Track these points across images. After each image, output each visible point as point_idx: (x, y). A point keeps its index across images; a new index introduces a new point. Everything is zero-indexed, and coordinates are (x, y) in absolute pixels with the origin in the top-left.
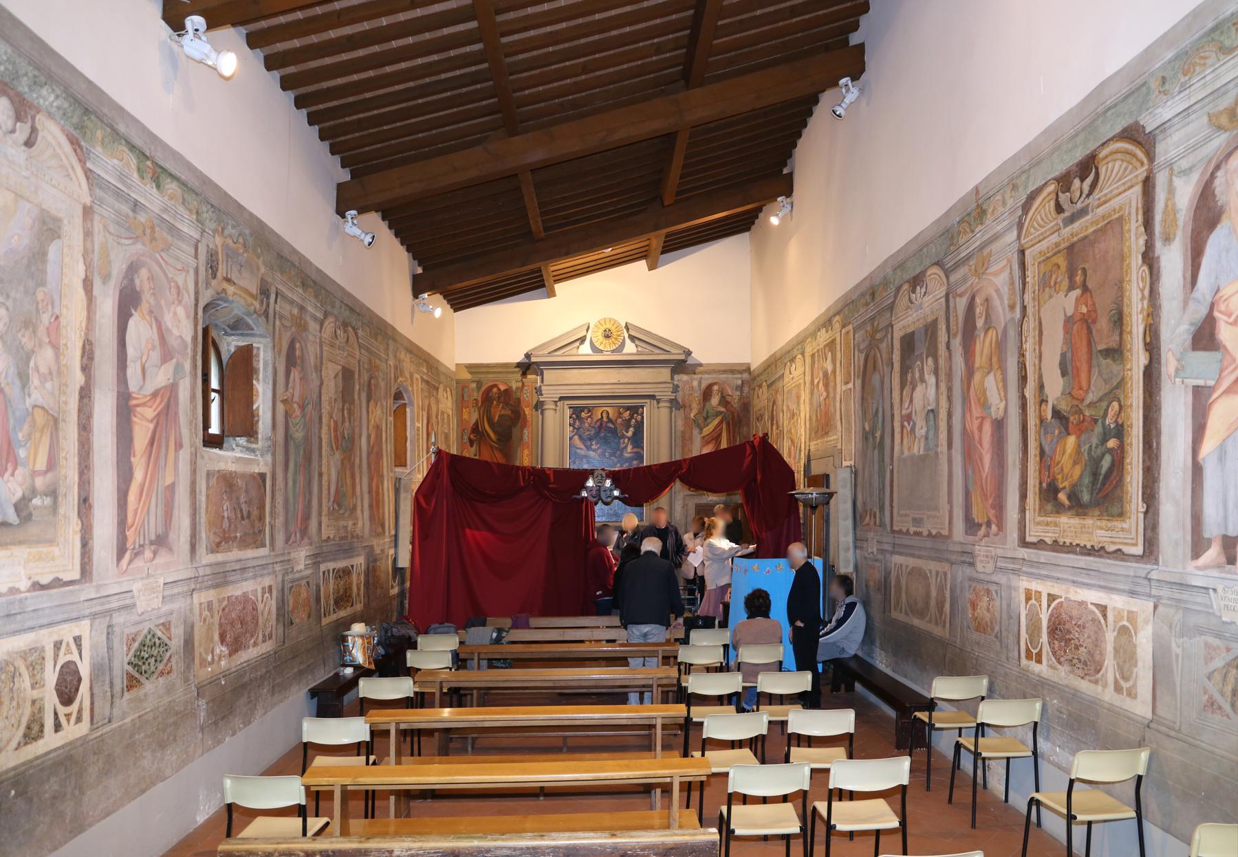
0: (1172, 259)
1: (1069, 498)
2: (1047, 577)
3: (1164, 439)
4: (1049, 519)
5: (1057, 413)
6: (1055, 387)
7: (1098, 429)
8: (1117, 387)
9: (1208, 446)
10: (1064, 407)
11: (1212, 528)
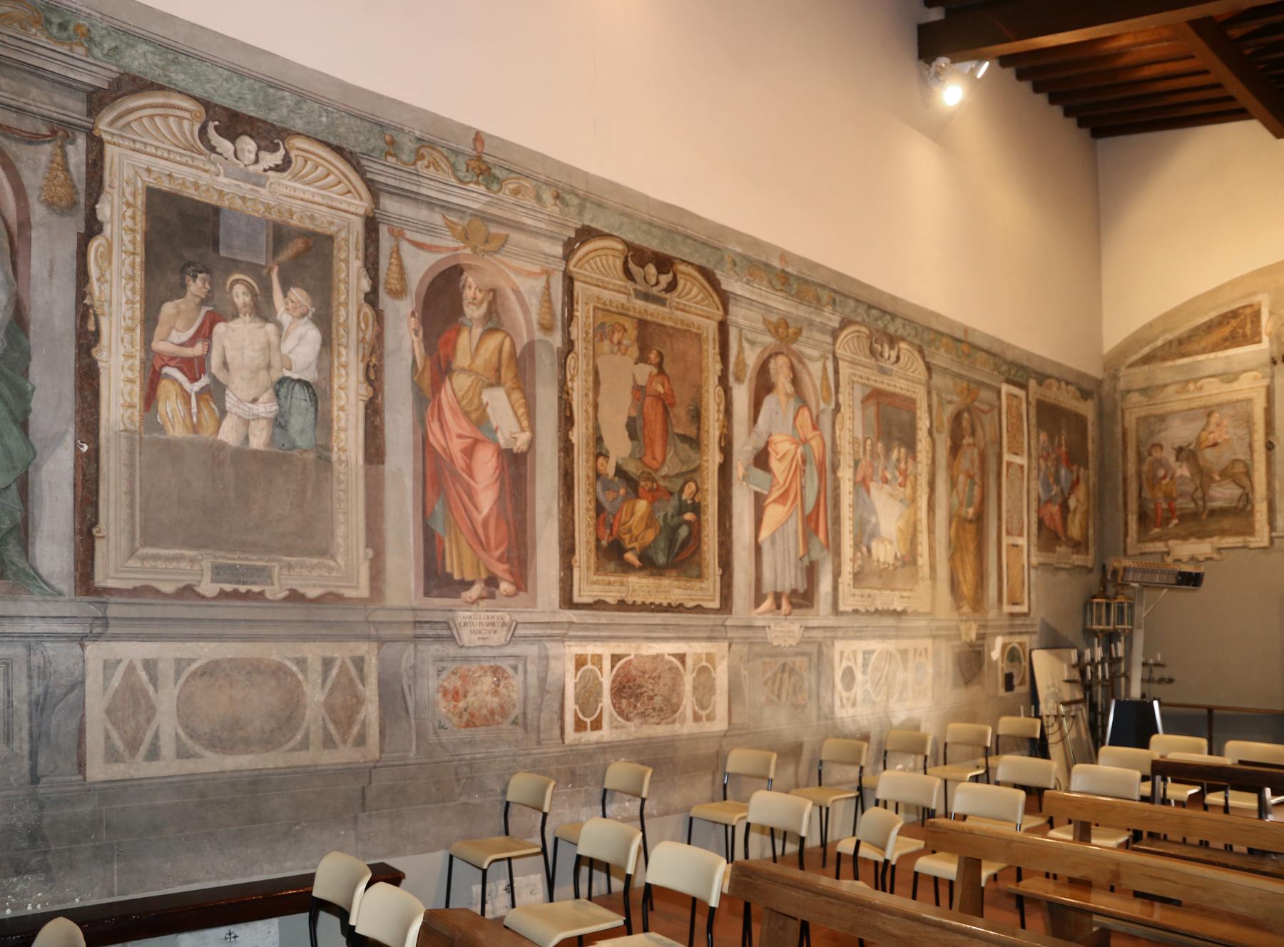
0: (742, 395)
1: (640, 558)
2: (611, 638)
3: (735, 522)
4: (612, 579)
5: (620, 471)
6: (619, 447)
7: (674, 502)
8: (694, 470)
9: (764, 534)
10: (632, 468)
11: (767, 588)
